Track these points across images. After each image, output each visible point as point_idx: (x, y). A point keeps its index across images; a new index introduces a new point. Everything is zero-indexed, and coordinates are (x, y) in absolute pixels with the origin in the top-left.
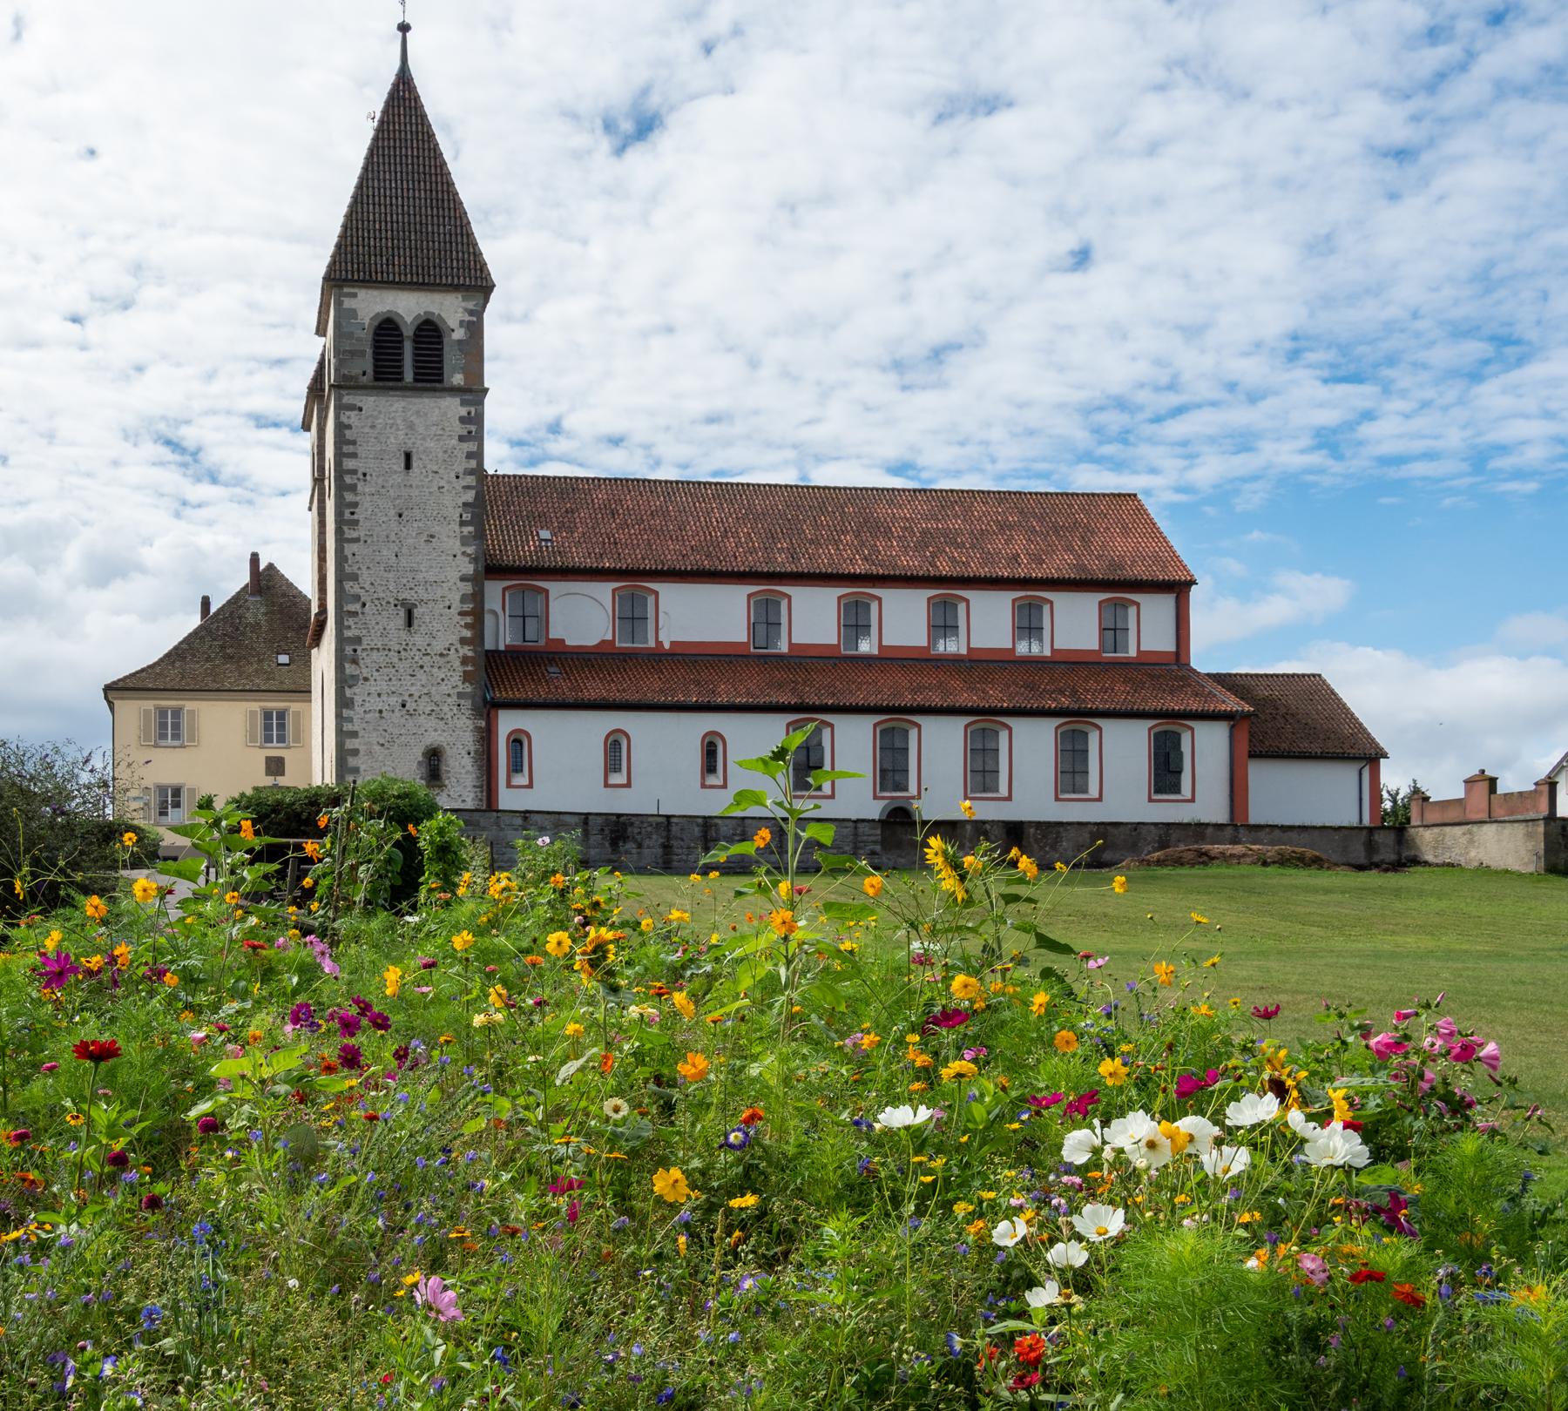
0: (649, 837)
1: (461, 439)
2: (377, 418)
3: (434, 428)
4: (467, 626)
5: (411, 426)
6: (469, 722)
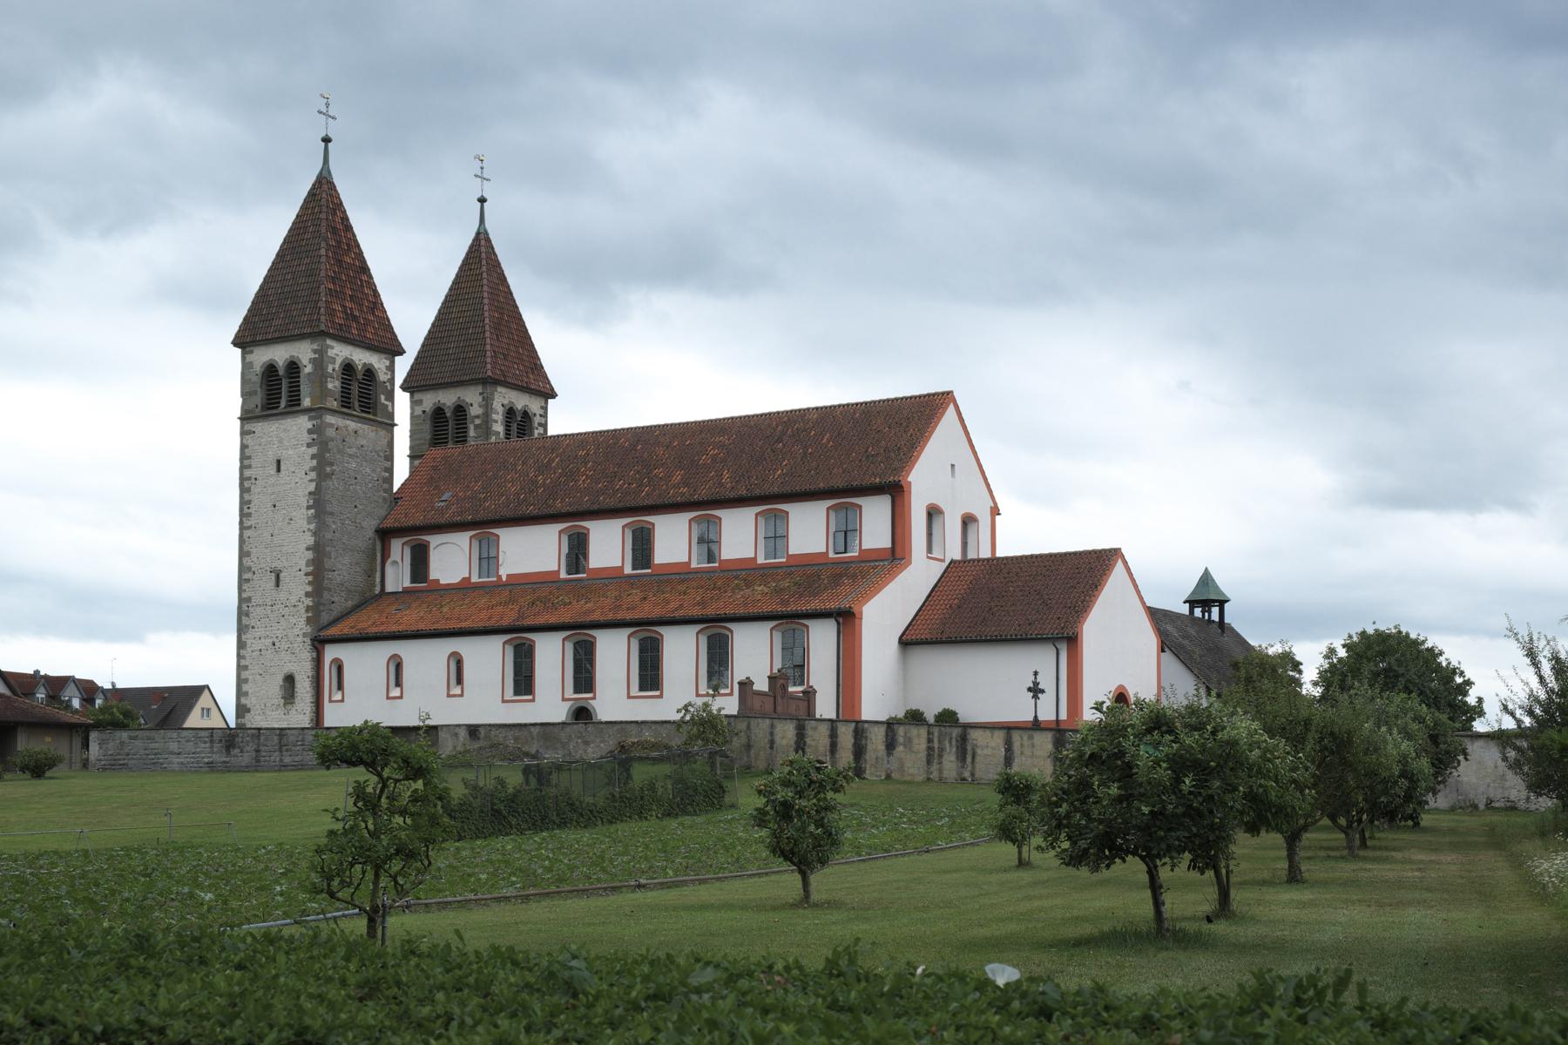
0: (248, 742)
1: (309, 445)
4: (310, 583)
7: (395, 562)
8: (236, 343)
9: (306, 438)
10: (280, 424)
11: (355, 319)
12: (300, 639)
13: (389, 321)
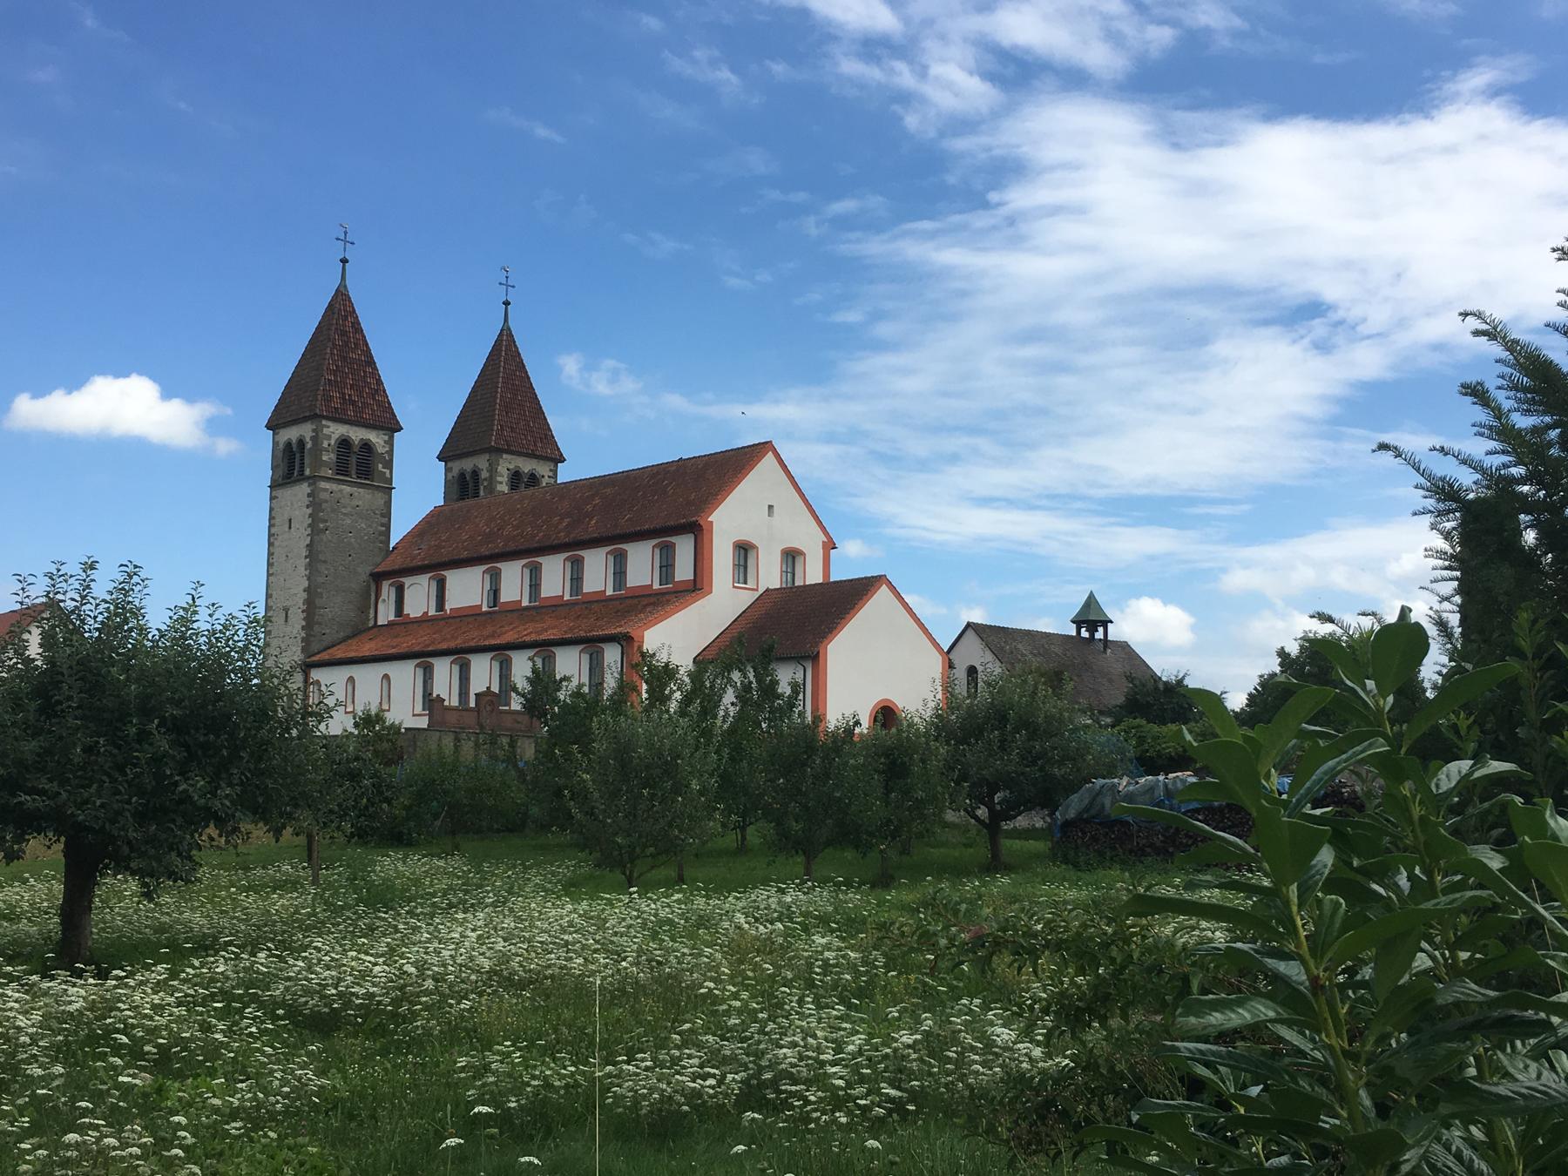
1: (308, 507)
4: (304, 619)
7: (384, 600)
8: (268, 427)
9: (306, 501)
11: (353, 403)
13: (389, 404)
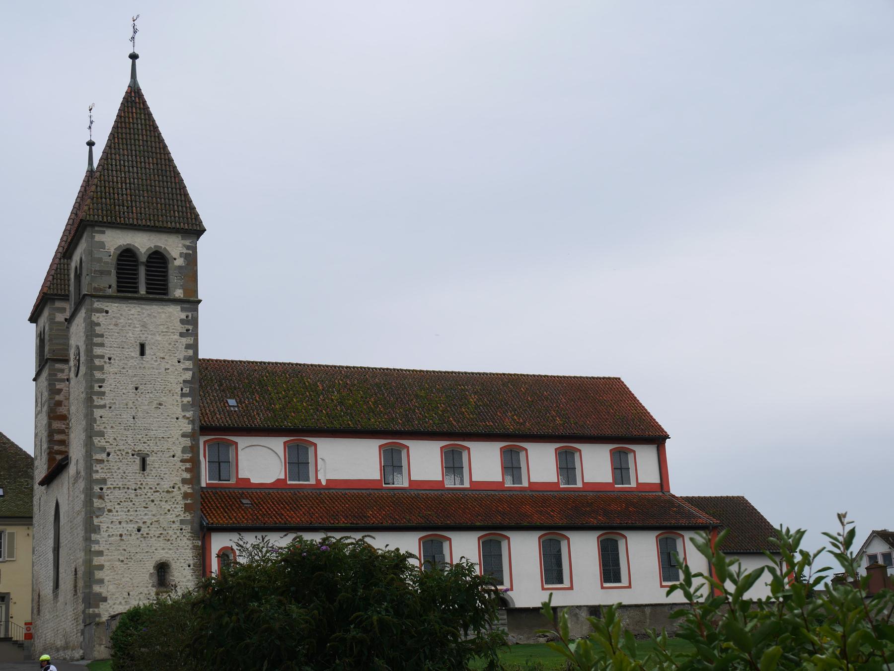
1: (182, 335)
2: (120, 319)
3: (162, 327)
4: (187, 470)
5: (144, 326)
6: (189, 542)
10: (142, 309)
12: (177, 525)
